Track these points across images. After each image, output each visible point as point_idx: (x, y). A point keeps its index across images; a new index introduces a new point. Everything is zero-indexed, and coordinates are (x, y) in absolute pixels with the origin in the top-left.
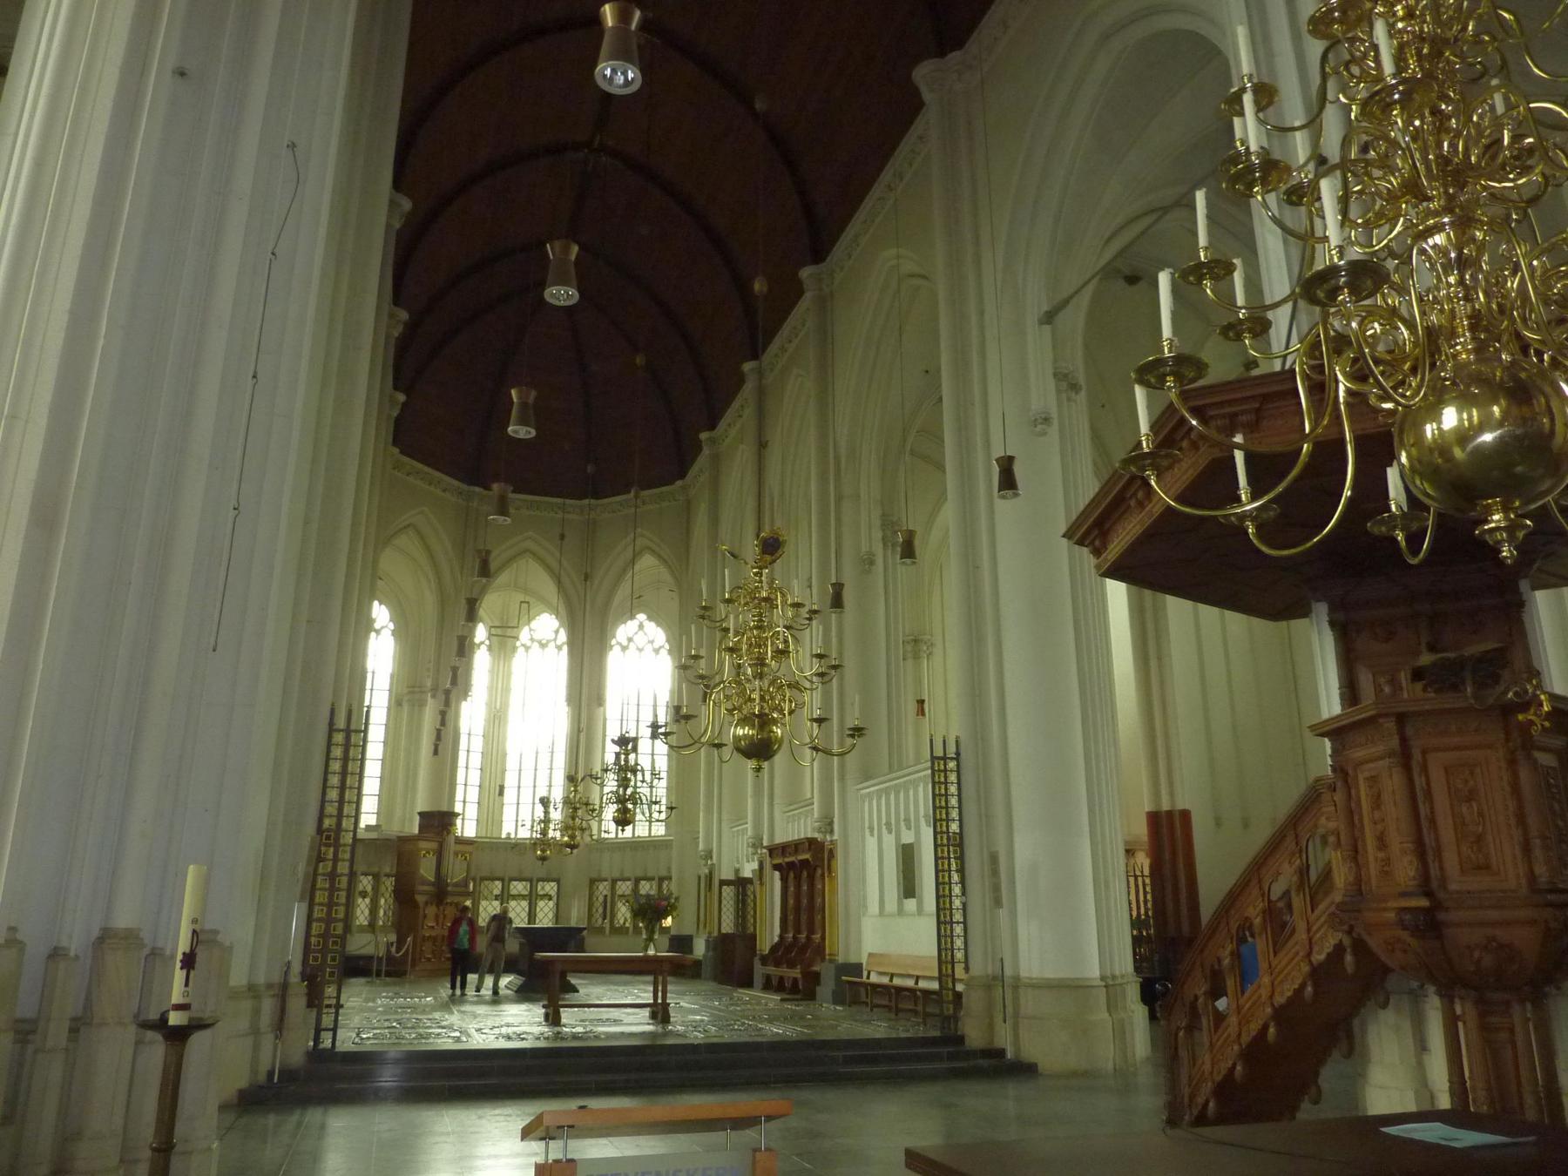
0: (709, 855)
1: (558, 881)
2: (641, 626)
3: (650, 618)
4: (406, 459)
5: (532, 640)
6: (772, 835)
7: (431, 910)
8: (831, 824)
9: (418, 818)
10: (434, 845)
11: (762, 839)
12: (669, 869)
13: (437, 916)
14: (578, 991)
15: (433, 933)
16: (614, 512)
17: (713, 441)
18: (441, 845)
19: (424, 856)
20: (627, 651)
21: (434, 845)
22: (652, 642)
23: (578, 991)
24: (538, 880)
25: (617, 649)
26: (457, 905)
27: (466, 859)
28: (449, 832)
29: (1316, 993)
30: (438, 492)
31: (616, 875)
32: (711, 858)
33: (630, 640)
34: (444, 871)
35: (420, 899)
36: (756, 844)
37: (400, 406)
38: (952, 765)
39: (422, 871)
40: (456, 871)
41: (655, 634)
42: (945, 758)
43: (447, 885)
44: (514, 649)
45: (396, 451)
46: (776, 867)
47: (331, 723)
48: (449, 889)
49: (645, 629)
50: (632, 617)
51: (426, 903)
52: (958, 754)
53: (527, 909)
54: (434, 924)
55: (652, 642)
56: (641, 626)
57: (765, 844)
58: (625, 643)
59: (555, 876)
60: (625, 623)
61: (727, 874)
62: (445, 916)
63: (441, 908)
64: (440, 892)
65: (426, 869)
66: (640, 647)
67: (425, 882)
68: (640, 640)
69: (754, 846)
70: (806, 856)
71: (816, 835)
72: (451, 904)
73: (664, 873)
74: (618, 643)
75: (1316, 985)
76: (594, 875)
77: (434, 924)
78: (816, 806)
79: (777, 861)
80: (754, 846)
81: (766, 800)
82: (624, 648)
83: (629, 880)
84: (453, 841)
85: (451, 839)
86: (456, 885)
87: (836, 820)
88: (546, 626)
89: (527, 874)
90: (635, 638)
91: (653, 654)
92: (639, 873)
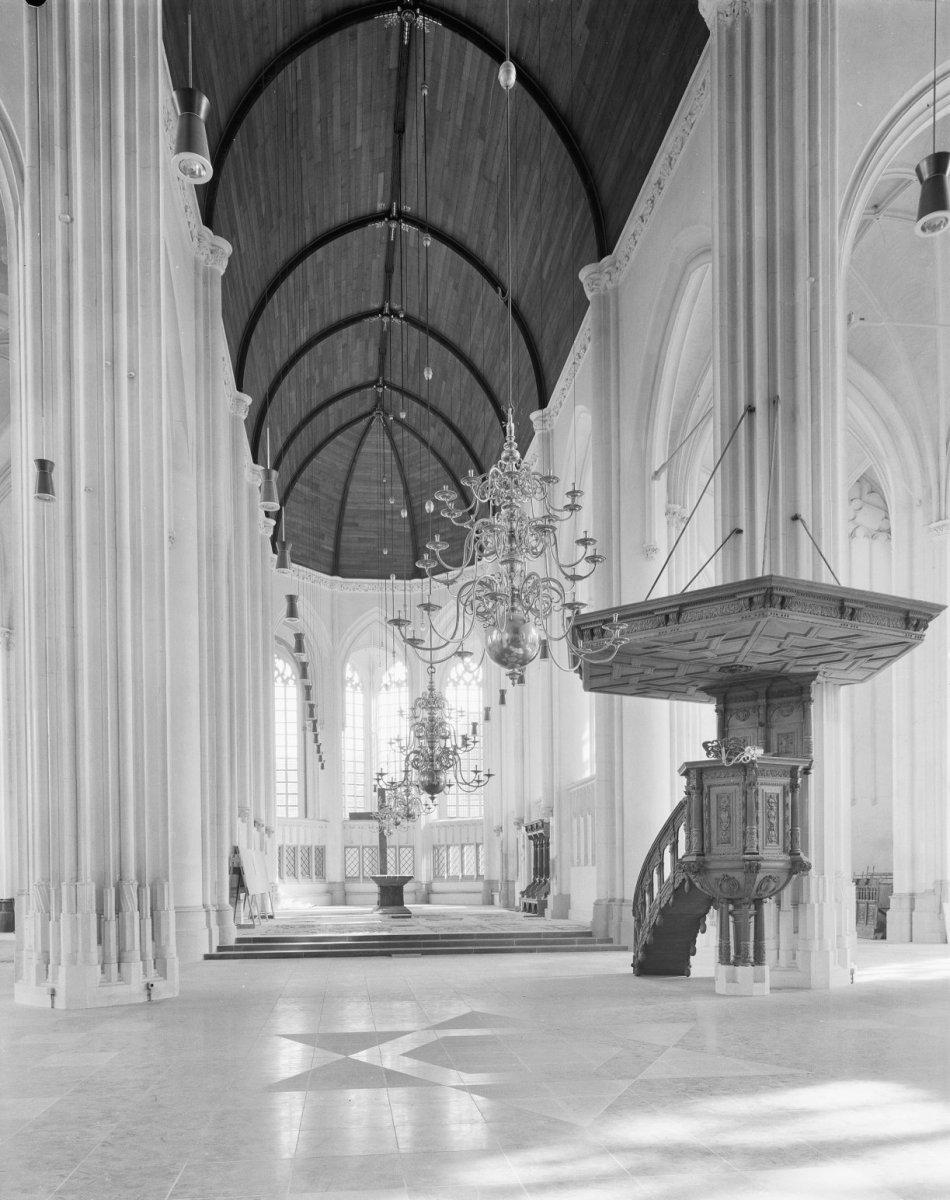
6: (529, 818)
8: (552, 811)
29: (673, 903)
33: (460, 678)
70: (541, 831)
74: (453, 680)
75: (674, 898)
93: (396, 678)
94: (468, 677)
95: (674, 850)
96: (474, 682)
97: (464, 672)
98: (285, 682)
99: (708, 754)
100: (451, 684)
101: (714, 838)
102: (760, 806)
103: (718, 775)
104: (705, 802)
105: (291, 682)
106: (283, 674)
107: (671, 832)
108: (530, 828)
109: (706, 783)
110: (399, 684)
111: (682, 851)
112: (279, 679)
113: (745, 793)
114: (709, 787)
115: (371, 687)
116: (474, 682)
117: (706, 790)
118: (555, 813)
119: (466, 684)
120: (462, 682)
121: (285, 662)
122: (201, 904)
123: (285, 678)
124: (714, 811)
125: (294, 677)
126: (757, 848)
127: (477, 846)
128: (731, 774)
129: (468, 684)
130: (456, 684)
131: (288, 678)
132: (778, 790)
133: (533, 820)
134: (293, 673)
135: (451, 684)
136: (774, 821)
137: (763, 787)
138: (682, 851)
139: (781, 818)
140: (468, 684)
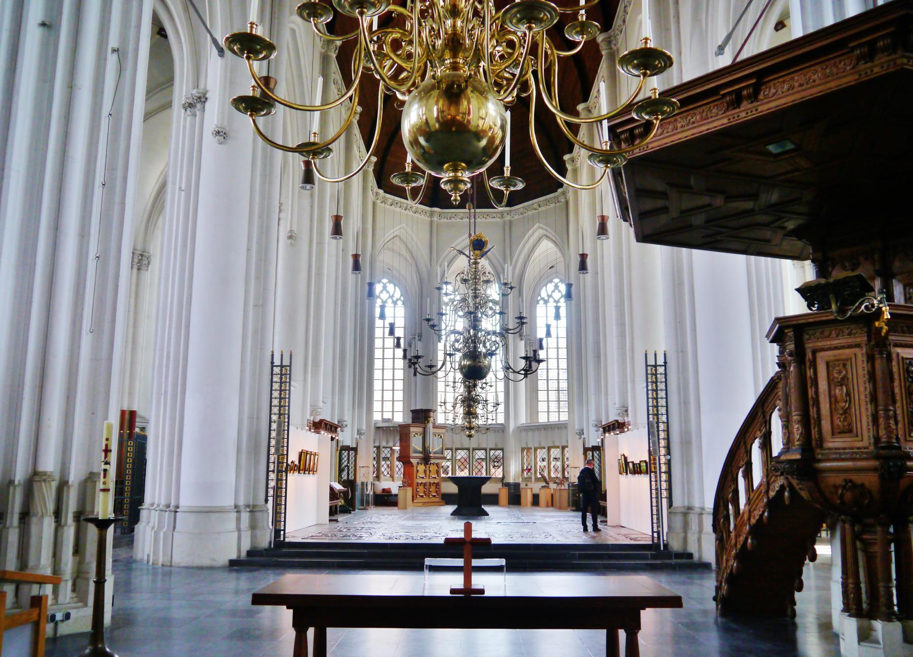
0: (581, 433)
1: (502, 450)
4: (388, 196)
7: (421, 468)
8: (627, 411)
9: (411, 414)
10: (420, 430)
11: (601, 421)
13: (425, 471)
14: (488, 515)
15: (424, 481)
16: (522, 214)
17: (573, 160)
18: (425, 429)
19: (414, 436)
20: (549, 304)
21: (420, 430)
23: (488, 515)
24: (491, 449)
26: (437, 465)
27: (441, 437)
30: (411, 213)
31: (537, 445)
32: (583, 434)
33: (549, 296)
34: (427, 445)
35: (414, 461)
37: (373, 165)
39: (413, 445)
40: (435, 445)
42: (655, 366)
43: (430, 453)
45: (381, 191)
47: (272, 363)
48: (431, 455)
50: (551, 281)
51: (418, 463)
52: (665, 362)
54: (423, 476)
59: (499, 446)
62: (430, 471)
63: (428, 466)
64: (426, 459)
65: (416, 443)
67: (416, 451)
69: (596, 426)
71: (617, 418)
72: (433, 464)
73: (564, 444)
76: (524, 446)
77: (423, 476)
80: (596, 426)
81: (603, 397)
83: (544, 448)
84: (431, 427)
85: (430, 425)
86: (435, 453)
89: (484, 446)
90: (554, 295)
92: (550, 445)
97: (553, 291)
98: (395, 303)
99: (810, 306)
100: (541, 302)
101: (826, 425)
102: (896, 376)
103: (827, 333)
104: (810, 373)
105: (400, 303)
106: (393, 296)
107: (760, 419)
109: (809, 346)
111: (777, 446)
112: (390, 301)
113: (871, 358)
114: (814, 352)
117: (809, 355)
119: (555, 301)
120: (551, 300)
121: (395, 286)
122: (232, 504)
123: (395, 299)
124: (823, 385)
125: (402, 298)
126: (898, 439)
127: (563, 448)
128: (847, 332)
130: (546, 302)
131: (397, 300)
134: (402, 295)
135: (541, 302)
137: (899, 350)
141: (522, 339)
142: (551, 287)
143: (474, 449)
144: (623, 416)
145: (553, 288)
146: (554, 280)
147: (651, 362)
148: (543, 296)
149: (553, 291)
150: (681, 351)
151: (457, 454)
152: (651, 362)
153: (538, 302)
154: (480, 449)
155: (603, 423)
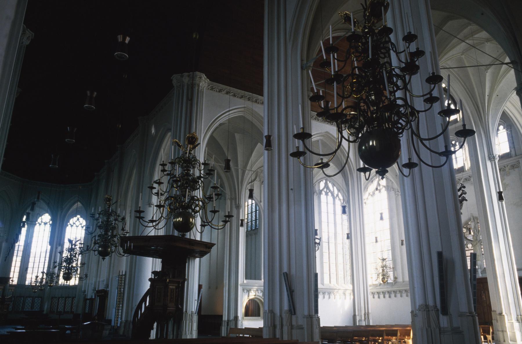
0: (85, 291)
2: (78, 219)
3: (81, 217)
5: (42, 222)
6: (99, 287)
8: (108, 286)
11: (96, 289)
12: (76, 295)
20: (73, 227)
22: (81, 224)
25: (69, 226)
28: (7, 283)
36: (94, 289)
38: (124, 277)
41: (84, 222)
42: (122, 275)
44: (36, 224)
46: (98, 296)
48: (6, 300)
49: (80, 220)
50: (76, 216)
53: (31, 306)
55: (81, 224)
56: (78, 219)
57: (97, 290)
58: (72, 224)
60: (73, 218)
61: (89, 297)
66: (77, 225)
68: (78, 223)
69: (94, 290)
78: (105, 282)
79: (98, 294)
82: (72, 226)
83: (64, 297)
87: (109, 285)
88: (46, 217)
90: (76, 223)
91: (81, 228)
93: (44, 221)
94: (78, 223)
95: (145, 304)
96: (80, 226)
97: (76, 221)
108: (98, 292)
110: (45, 224)
111: (147, 304)
115: (32, 223)
116: (80, 226)
118: (109, 287)
120: (74, 225)
127: (73, 298)
129: (77, 226)
130: (72, 226)
132: (174, 287)
133: (100, 289)
136: (172, 296)
137: (170, 287)
138: (147, 304)
139: (174, 295)
140: (77, 226)
141: (60, 246)
142: (75, 219)
143: (27, 297)
144: (106, 288)
145: (76, 220)
146: (77, 216)
147: (121, 274)
148: (70, 223)
149: (76, 221)
150: (131, 271)
151: (35, 300)
152: (121, 274)
153: (67, 225)
154: (29, 297)
155: (97, 290)
